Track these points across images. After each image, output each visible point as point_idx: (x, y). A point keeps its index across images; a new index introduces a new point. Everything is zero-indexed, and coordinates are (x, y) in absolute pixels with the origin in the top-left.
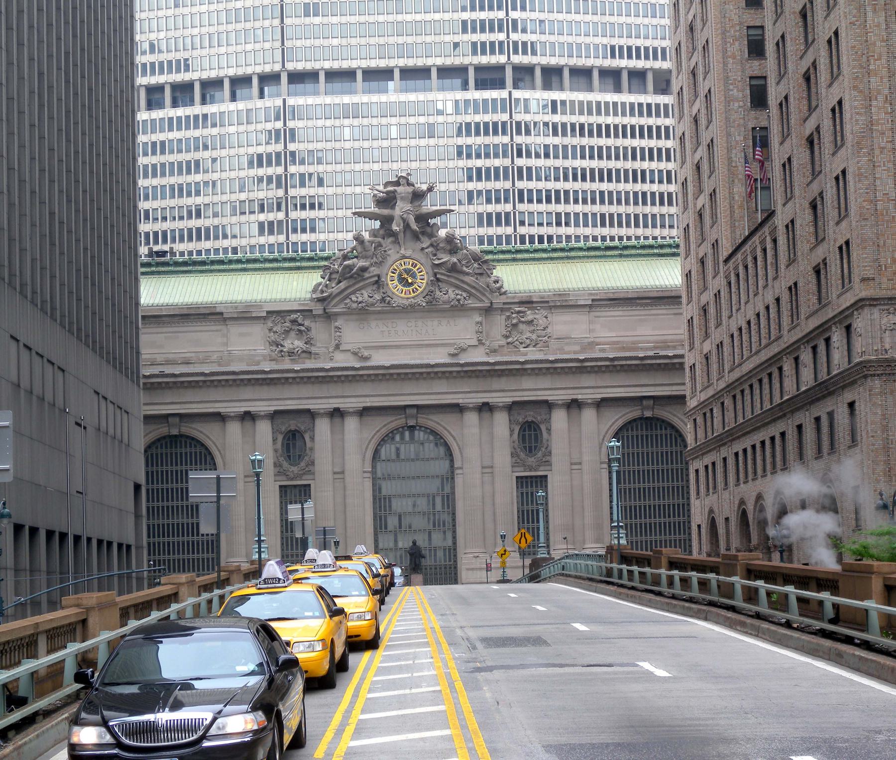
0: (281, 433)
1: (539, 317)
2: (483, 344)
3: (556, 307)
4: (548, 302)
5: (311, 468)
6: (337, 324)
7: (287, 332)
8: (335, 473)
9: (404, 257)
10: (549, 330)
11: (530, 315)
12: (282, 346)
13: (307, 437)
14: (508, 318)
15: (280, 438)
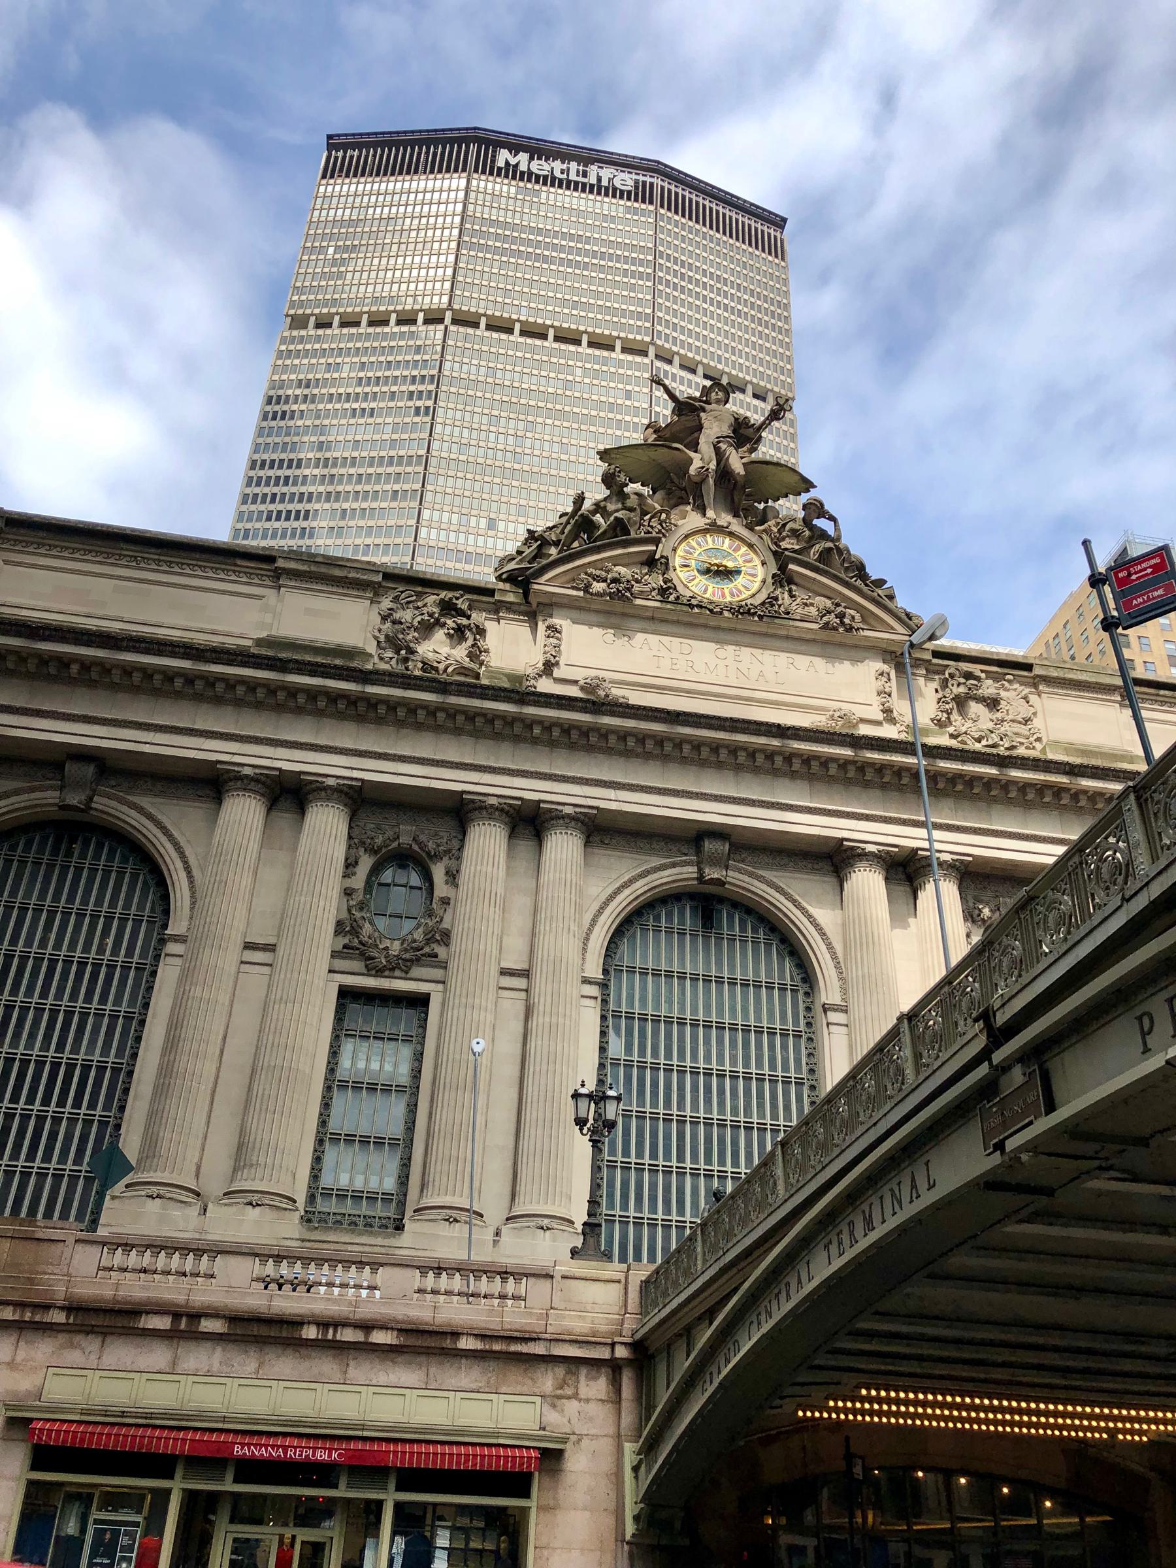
0: (373, 851)
1: (1012, 694)
2: (892, 721)
3: (1048, 680)
4: (1028, 667)
5: (441, 951)
6: (556, 621)
7: (427, 628)
8: (504, 972)
9: (714, 528)
10: (1037, 723)
11: (989, 688)
12: (412, 651)
13: (438, 872)
14: (944, 684)
15: (366, 863)
